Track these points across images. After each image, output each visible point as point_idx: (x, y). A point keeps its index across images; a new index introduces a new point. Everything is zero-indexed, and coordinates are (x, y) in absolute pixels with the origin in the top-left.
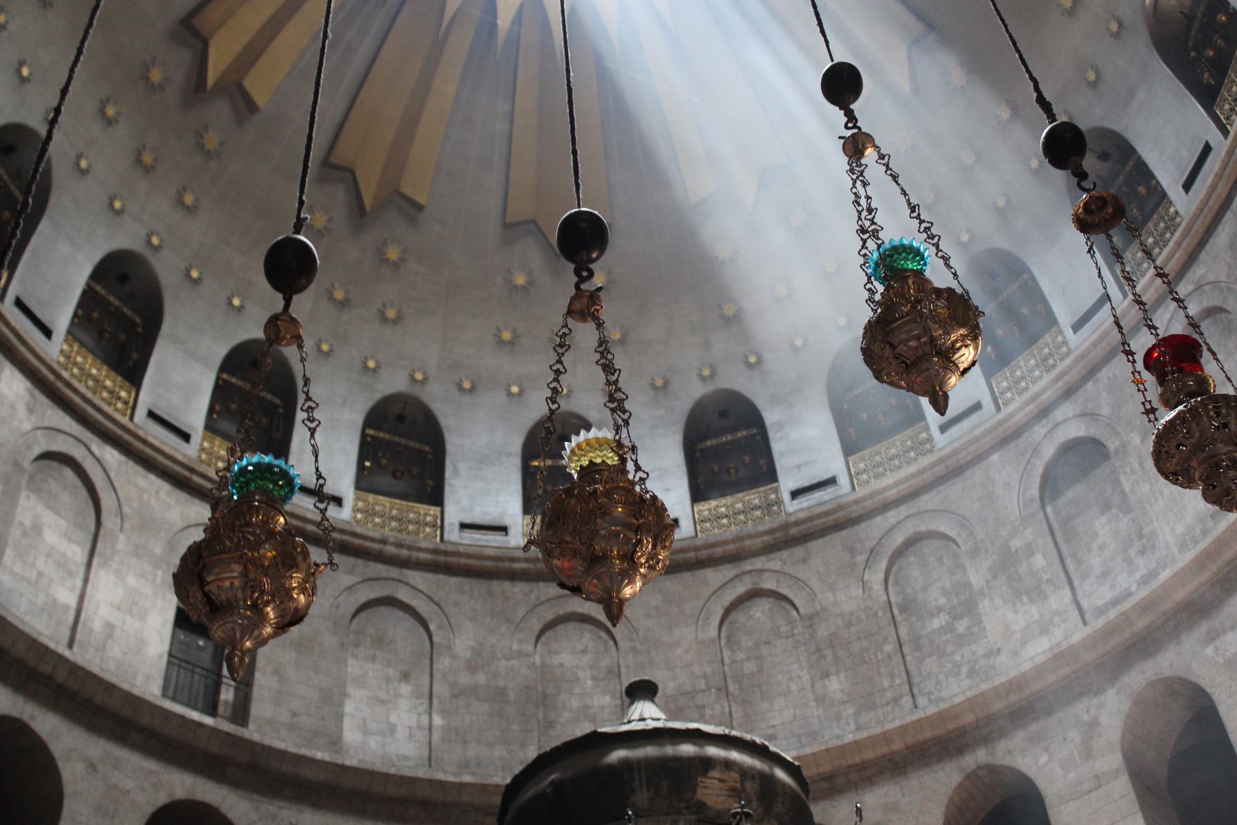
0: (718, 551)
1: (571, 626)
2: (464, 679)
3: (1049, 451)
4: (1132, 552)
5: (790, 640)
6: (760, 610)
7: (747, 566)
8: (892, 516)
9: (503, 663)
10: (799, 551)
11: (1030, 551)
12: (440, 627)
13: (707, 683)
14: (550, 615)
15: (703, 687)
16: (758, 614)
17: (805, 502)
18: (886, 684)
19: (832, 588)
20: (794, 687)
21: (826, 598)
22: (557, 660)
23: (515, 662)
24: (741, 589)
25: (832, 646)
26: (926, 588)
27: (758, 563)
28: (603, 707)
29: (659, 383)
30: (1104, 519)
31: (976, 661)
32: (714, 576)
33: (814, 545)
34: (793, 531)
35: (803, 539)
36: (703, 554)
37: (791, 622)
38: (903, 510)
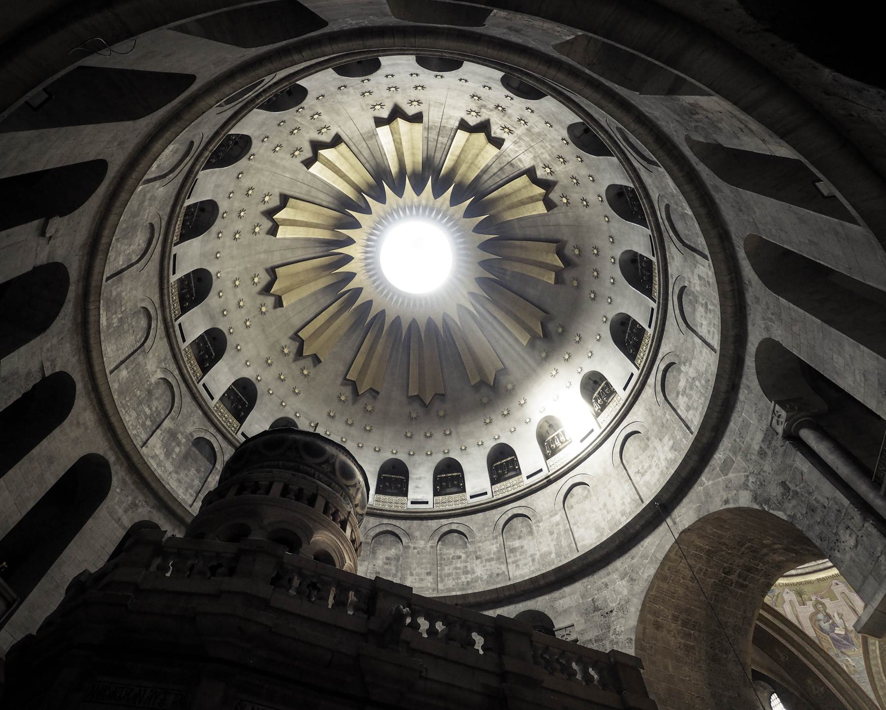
0: (166, 298)
1: (148, 236)
2: (148, 196)
3: (207, 437)
4: (190, 491)
6: (143, 323)
7: (159, 312)
8: (176, 372)
9: (147, 212)
10: (164, 334)
11: (179, 444)
12: (170, 178)
14: (156, 226)
16: (142, 322)
17: (177, 328)
18: (127, 399)
19: (154, 355)
20: (120, 352)
21: (150, 355)
22: (139, 233)
23: (146, 217)
24: (152, 311)
26: (157, 399)
27: (160, 317)
28: (119, 262)
29: (218, 255)
30: (195, 472)
31: (139, 436)
32: (156, 298)
33: (165, 340)
34: (171, 330)
35: (168, 335)
36: (166, 291)
37: (140, 339)
38: (179, 377)
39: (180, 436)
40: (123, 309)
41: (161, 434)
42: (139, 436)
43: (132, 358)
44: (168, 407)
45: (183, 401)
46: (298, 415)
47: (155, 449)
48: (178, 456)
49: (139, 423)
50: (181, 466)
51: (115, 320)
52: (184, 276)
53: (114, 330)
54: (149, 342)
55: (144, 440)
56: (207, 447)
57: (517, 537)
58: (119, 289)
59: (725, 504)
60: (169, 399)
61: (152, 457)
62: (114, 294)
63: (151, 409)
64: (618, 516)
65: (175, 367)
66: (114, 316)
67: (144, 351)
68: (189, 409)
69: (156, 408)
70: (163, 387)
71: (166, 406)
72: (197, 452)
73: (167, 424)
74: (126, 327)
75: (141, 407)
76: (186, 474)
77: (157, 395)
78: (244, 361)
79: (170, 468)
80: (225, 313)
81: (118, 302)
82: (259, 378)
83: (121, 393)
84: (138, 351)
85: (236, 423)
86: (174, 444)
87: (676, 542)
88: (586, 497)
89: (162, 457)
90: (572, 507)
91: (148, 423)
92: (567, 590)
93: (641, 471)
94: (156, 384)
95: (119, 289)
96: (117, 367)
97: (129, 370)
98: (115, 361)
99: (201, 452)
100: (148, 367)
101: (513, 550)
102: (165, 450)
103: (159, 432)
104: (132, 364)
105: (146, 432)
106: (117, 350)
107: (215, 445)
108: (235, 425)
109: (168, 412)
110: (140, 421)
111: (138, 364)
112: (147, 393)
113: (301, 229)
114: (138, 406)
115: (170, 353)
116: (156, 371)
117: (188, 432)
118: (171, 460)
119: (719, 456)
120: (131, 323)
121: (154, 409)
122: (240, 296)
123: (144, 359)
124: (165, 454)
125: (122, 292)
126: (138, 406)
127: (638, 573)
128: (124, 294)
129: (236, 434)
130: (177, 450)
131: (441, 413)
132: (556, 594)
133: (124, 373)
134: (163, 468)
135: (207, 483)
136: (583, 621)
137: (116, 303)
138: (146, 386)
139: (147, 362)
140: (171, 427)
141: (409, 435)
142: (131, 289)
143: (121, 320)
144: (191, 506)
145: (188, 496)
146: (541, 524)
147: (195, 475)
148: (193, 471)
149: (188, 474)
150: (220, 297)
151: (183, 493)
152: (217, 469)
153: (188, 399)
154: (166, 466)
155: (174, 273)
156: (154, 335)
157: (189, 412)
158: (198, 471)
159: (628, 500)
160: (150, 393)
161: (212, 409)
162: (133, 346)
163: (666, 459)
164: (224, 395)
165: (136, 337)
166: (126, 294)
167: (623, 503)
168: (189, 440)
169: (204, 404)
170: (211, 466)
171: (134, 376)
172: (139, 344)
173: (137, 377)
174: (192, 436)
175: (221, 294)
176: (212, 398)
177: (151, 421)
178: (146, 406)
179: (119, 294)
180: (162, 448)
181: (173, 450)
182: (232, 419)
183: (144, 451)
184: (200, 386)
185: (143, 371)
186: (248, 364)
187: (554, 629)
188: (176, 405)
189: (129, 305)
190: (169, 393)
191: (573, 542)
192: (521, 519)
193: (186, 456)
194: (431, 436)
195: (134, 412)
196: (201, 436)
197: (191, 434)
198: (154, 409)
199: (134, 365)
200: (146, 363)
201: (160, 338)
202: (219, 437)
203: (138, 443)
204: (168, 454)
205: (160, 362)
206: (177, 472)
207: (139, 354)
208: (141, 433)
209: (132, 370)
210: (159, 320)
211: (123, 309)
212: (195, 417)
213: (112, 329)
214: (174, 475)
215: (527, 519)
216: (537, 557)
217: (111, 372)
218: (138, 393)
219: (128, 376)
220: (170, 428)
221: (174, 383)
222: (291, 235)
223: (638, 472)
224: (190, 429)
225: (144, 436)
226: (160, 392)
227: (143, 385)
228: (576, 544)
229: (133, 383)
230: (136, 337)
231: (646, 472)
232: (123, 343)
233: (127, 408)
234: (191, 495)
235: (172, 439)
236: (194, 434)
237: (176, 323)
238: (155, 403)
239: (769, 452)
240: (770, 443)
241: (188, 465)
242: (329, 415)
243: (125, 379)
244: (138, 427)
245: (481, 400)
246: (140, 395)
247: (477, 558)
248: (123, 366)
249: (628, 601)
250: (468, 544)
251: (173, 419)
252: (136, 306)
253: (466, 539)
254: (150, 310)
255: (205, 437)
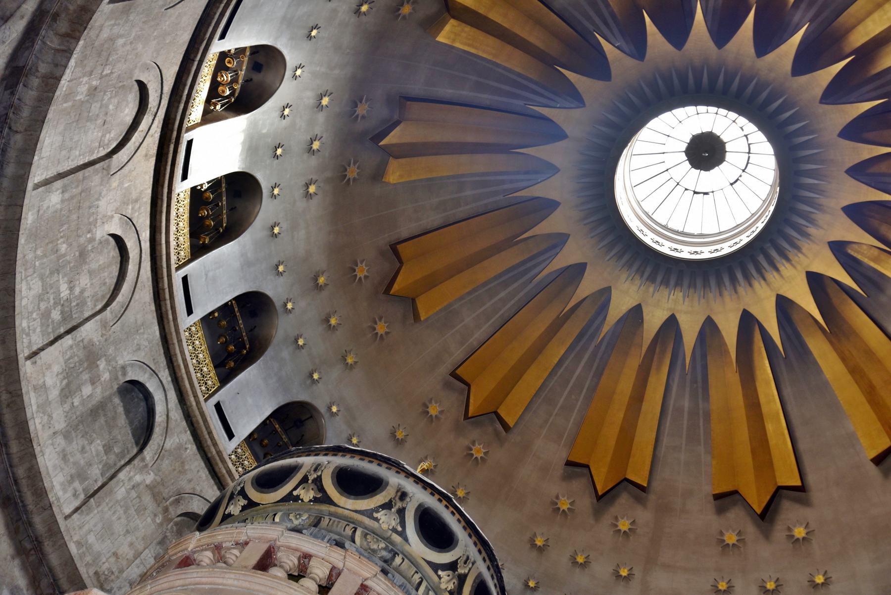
3: (152, 386)
4: (77, 484)
5: (97, 144)
8: (145, 235)
10: (154, 150)
13: (107, 75)
15: (105, 73)
18: (39, 252)
19: (121, 183)
20: (64, 153)
21: (115, 182)
25: (82, 191)
29: (314, 33)
30: (101, 448)
31: (28, 335)
33: (153, 161)
38: (146, 246)
39: (102, 364)
40: (107, 71)
41: (71, 347)
42: (28, 335)
43: (80, 174)
44: (103, 296)
45: (136, 296)
46: (334, 409)
47: (48, 374)
48: (83, 403)
49: (39, 308)
50: (81, 427)
51: (83, 89)
52: (236, 49)
53: (73, 106)
54: (123, 155)
55: (35, 348)
56: (142, 407)
58: (116, 30)
60: (111, 282)
61: (35, 388)
62: (105, 35)
63: (71, 289)
65: (148, 222)
66: (85, 79)
67: (109, 167)
68: (139, 316)
69: (82, 291)
70: (113, 252)
71: (100, 294)
72: (121, 409)
73: (89, 331)
74: (95, 107)
75: (55, 278)
76: (83, 448)
77: (94, 266)
78: (275, 261)
79: (60, 424)
80: (279, 151)
81: (105, 54)
82: (290, 306)
83: (34, 236)
84: (97, 166)
85: (212, 380)
86: (85, 376)
89: (54, 394)
91: (56, 315)
94: (101, 243)
95: (116, 30)
96: (47, 182)
97: (67, 196)
98: (47, 168)
99: (127, 411)
100: (102, 203)
102: (65, 382)
103: (68, 341)
104: (77, 186)
105: (44, 333)
106: (62, 147)
107: (159, 409)
108: (210, 383)
109: (99, 307)
110: (43, 306)
111: (86, 191)
112: (77, 254)
113: (491, 40)
114: (52, 273)
115: (149, 191)
116: (112, 217)
117: (121, 362)
118: (67, 407)
120: (107, 106)
121: (77, 291)
122: (318, 130)
123: (101, 184)
124: (62, 390)
125: (120, 36)
126: (52, 273)
128: (120, 41)
129: (206, 400)
130: (87, 390)
131: (624, 525)
133: (55, 198)
134: (46, 417)
135: (115, 480)
137: (99, 55)
138: (82, 240)
139: (104, 193)
140: (95, 340)
141: (539, 542)
142: (138, 38)
143: (93, 92)
144: (67, 517)
145: (69, 494)
147: (97, 455)
148: (97, 446)
149: (87, 448)
150: (283, 116)
151: (62, 484)
152: (143, 460)
153: (145, 294)
154: (54, 416)
155: (222, 37)
156: (137, 144)
157: (139, 322)
158: (108, 449)
160: (83, 254)
161: (181, 331)
162: (92, 152)
164: (212, 313)
165: (104, 136)
166: (124, 45)
168: (116, 378)
169: (171, 317)
170: (135, 450)
171: (70, 211)
172: (102, 153)
173: (74, 217)
174: (124, 374)
175: (287, 111)
176: (190, 311)
177: (62, 312)
178: (66, 279)
179: (112, 40)
180: (61, 376)
181: (79, 388)
182: (208, 368)
183: (27, 368)
184: (177, 277)
185: (90, 207)
186: (281, 268)
188: (120, 298)
189: (121, 67)
190: (115, 270)
193: (97, 410)
194: (584, 565)
195: (40, 284)
196: (141, 380)
197: (123, 368)
198: (77, 291)
199: (80, 188)
200: (100, 194)
201: (146, 155)
202: (172, 395)
203: (23, 351)
204: (67, 393)
205: (125, 203)
206: (67, 436)
207: (97, 172)
208: (34, 330)
209: (72, 198)
210: (157, 119)
211: (107, 71)
212: (145, 336)
213: (70, 104)
214: (60, 440)
217: (37, 186)
218: (63, 248)
219: (59, 206)
220: (91, 340)
221: (133, 253)
222: (466, 44)
224: (125, 357)
225: (38, 341)
226: (101, 262)
227: (79, 236)
229: (62, 225)
230: (104, 136)
232: (76, 138)
233: (31, 271)
234: (75, 495)
235: (85, 365)
236: (129, 369)
237: (186, 137)
238: (84, 281)
241: (94, 431)
242: (393, 435)
243: (51, 210)
244: (34, 315)
245: (721, 533)
246: (64, 255)
248: (59, 184)
251: (104, 325)
252: (131, 73)
254: (150, 92)
255: (148, 385)
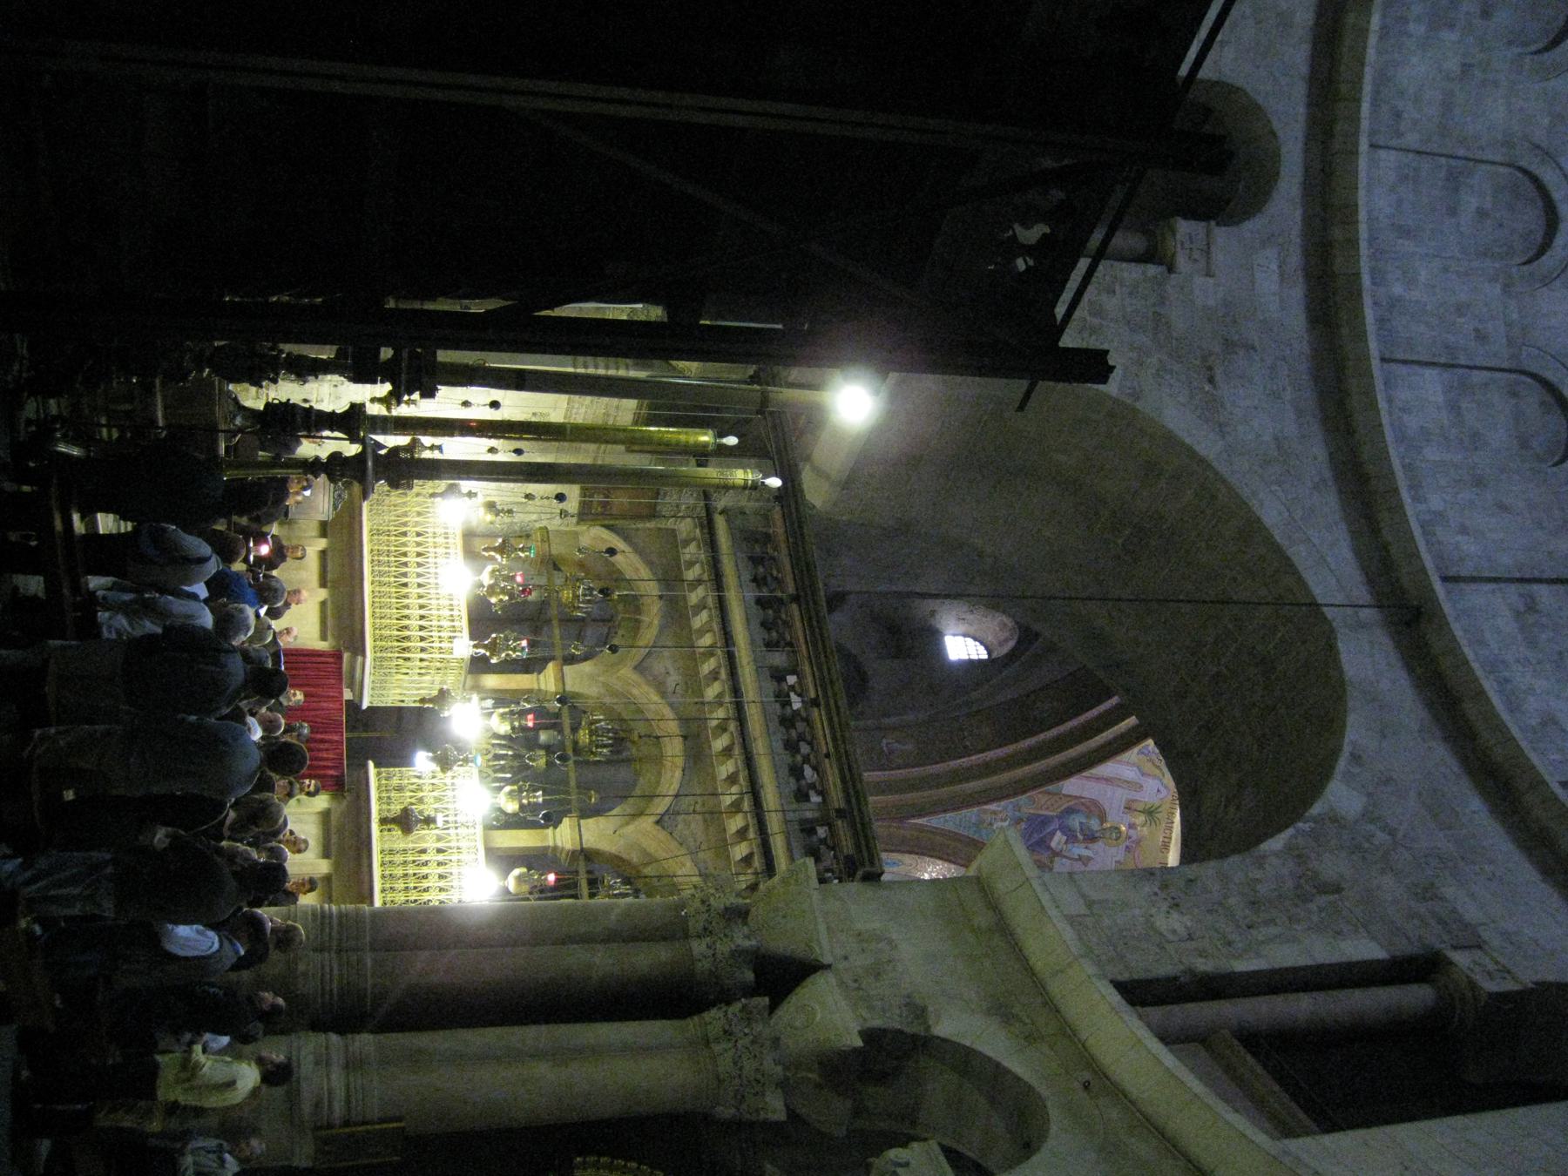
57: (1488, 206)
59: (1352, 754)
64: (1435, 502)
87: (1314, 606)
88: (1524, 444)
90: (1514, 394)
92: (1297, 292)
93: (1531, 619)
101: (1454, 181)
119: (1474, 807)
127: (1279, 483)
132: (1295, 259)
136: (1211, 302)
146: (1498, 289)
159: (1469, 546)
163: (1531, 690)
167: (1464, 530)
187: (1213, 223)
191: (1415, 358)
192: (1539, 237)
215: (1531, 254)
216: (1408, 246)
223: (1531, 606)
228: (1405, 362)
231: (1522, 629)
239: (1422, 908)
240: (1441, 921)
247: (1466, 67)
249: (1222, 429)
250: (1520, 50)
253: (1533, 48)
